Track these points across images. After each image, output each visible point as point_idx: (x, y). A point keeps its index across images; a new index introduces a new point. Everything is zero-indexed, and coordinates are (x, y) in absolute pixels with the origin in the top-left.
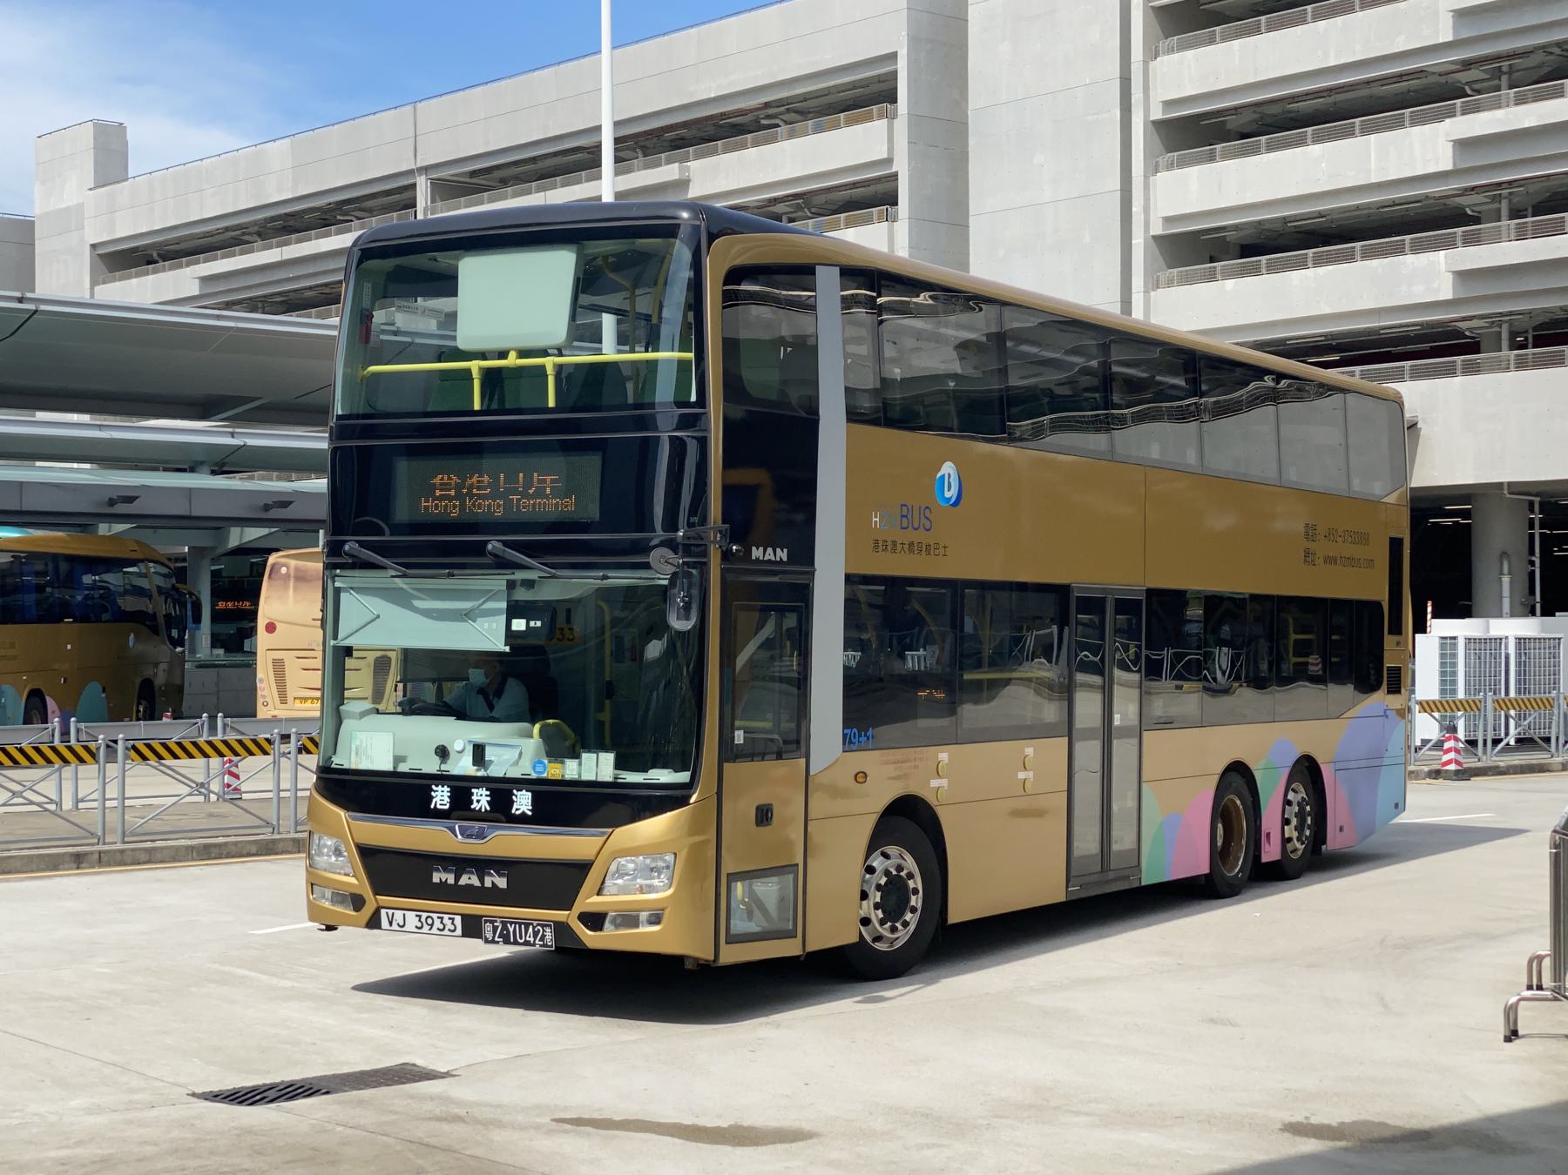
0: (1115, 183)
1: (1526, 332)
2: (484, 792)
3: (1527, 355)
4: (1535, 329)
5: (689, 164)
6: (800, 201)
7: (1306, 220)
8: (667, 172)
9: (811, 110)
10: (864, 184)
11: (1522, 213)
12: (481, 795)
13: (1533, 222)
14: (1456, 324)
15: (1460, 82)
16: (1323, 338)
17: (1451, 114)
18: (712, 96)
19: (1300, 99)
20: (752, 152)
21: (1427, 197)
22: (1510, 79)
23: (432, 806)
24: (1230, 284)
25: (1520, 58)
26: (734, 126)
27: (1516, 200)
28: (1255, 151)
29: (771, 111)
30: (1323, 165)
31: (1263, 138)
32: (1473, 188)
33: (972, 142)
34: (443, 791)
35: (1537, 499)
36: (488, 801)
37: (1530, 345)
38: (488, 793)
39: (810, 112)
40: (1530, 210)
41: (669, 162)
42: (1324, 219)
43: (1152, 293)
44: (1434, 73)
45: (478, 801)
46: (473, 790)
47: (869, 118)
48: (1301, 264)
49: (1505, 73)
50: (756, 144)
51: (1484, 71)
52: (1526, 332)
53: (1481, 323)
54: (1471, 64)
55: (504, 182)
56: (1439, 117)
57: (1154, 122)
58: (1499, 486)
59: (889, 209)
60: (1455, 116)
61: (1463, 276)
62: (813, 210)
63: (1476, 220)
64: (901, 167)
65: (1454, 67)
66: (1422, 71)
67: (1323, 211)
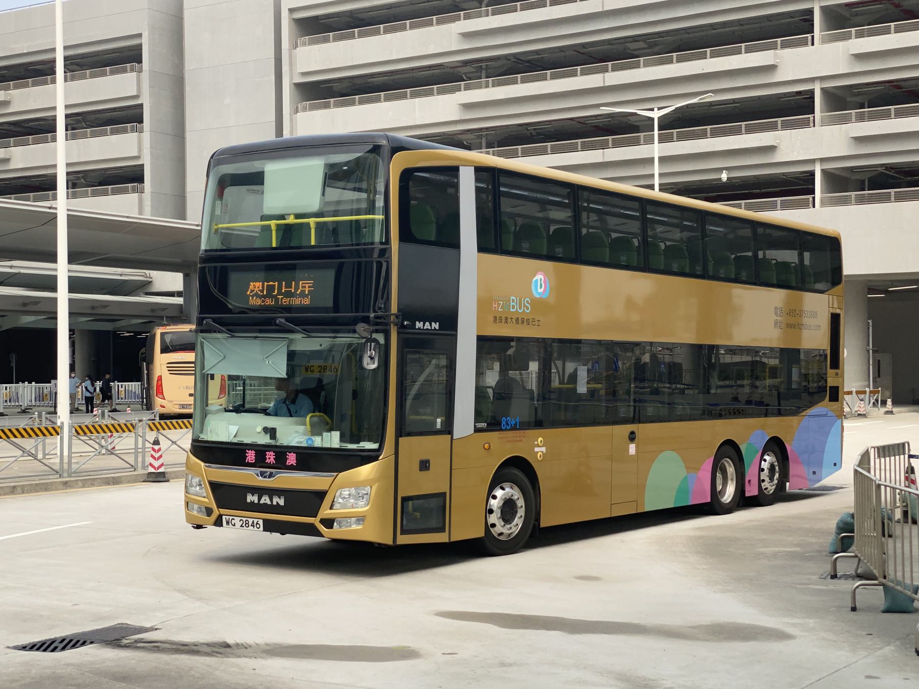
0: (272, 117)
2: (273, 454)
9: (86, 64)
10: (121, 109)
15: (460, 72)
21: (444, 134)
22: (486, 73)
28: (352, 103)
30: (390, 113)
32: (468, 130)
33: (188, 89)
36: (274, 458)
38: (274, 454)
40: (496, 143)
44: (447, 67)
45: (269, 458)
46: (267, 453)
47: (124, 71)
51: (474, 67)
54: (467, 63)
59: (138, 125)
60: (461, 91)
62: (88, 123)
64: (146, 101)
65: (459, 64)
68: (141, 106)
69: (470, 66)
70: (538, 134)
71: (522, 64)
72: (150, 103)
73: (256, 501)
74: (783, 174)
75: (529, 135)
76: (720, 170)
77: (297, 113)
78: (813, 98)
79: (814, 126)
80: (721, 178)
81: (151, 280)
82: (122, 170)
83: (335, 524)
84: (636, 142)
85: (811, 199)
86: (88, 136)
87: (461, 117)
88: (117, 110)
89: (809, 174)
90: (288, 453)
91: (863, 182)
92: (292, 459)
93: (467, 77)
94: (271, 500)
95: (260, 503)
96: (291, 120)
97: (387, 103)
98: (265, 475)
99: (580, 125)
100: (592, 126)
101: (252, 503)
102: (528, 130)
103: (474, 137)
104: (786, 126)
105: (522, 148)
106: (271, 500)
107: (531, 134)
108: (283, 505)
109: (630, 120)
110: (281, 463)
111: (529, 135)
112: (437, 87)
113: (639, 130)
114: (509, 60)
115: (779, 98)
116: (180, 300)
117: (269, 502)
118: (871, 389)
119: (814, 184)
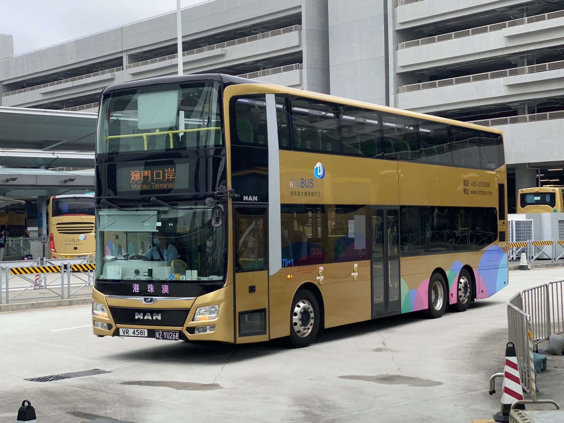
0: (383, 54)
1: (534, 107)
2: (152, 286)
3: (535, 115)
5: (225, 48)
6: (267, 62)
8: (217, 51)
10: (290, 55)
11: (532, 63)
12: (151, 287)
13: (536, 66)
14: (509, 104)
15: (508, 14)
16: (460, 111)
17: (504, 26)
18: (233, 22)
19: (450, 21)
20: (248, 43)
21: (496, 57)
22: (527, 13)
23: (133, 291)
25: (529, 5)
26: (241, 33)
28: (433, 41)
29: (254, 28)
31: (436, 36)
32: (514, 54)
34: (136, 286)
35: (539, 169)
37: (536, 112)
38: (153, 286)
39: (270, 28)
40: (535, 61)
41: (217, 48)
42: (459, 66)
43: (397, 95)
44: (498, 11)
46: (148, 285)
47: (291, 30)
48: (451, 83)
49: (525, 11)
50: (250, 40)
51: (517, 10)
52: (534, 107)
54: (513, 7)
55: (156, 56)
56: (500, 28)
57: (396, 31)
58: (524, 164)
59: (299, 64)
61: (511, 86)
62: (272, 65)
63: (515, 66)
64: (304, 49)
66: (495, 11)
68: (301, 52)
69: (514, 9)
71: (551, 5)
73: (142, 318)
75: (557, 54)
77: (398, 50)
83: (196, 330)
86: (270, 73)
88: (288, 55)
90: (162, 285)
92: (165, 289)
93: (513, 17)
94: (152, 317)
95: (146, 318)
98: (147, 300)
101: (139, 319)
102: (556, 51)
103: (519, 58)
105: (549, 64)
106: (152, 317)
107: (558, 53)
108: (160, 319)
110: (158, 293)
111: (557, 54)
112: (490, 26)
114: (541, 3)
117: (150, 318)
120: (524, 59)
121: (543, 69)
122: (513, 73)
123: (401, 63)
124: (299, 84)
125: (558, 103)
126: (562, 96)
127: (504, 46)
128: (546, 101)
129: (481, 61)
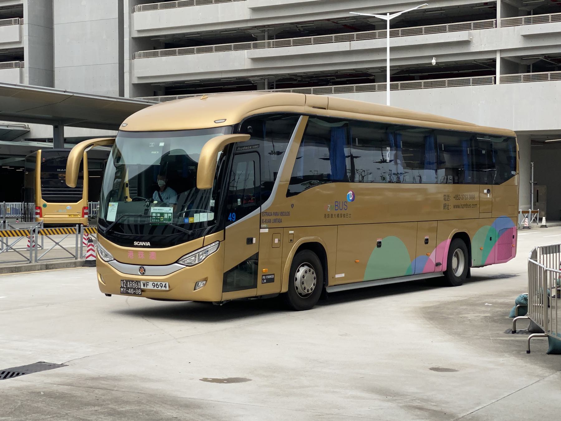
0: (116, 15)
1: (273, 82)
4: (276, 81)
7: (192, 35)
10: (6, 8)
21: (238, 29)
24: (164, 58)
27: (270, 32)
30: (200, 14)
32: (255, 27)
37: (275, 88)
40: (275, 36)
42: (199, 35)
43: (133, 60)
48: (192, 52)
52: (273, 82)
53: (258, 78)
59: (19, 19)
61: (255, 60)
63: (256, 39)
67: (199, 32)
70: (305, 30)
72: (28, 4)
74: (474, 60)
75: (298, 30)
76: (431, 57)
78: (496, 7)
79: (496, 27)
80: (432, 63)
81: (29, 130)
82: (7, 51)
84: (373, 37)
85: (493, 78)
87: (250, 17)
88: (5, 8)
89: (492, 61)
91: (529, 66)
96: (130, 18)
97: (198, 7)
99: (334, 24)
100: (342, 25)
102: (297, 27)
104: (477, 27)
107: (299, 29)
109: (368, 21)
113: (375, 28)
115: (472, 7)
116: (51, 145)
118: (533, 210)
119: (495, 68)
120: (265, 33)
121: (288, 44)
122: (255, 47)
123: (138, 26)
124: (18, 40)
125: (296, 80)
126: (305, 73)
127: (248, 17)
128: (288, 77)
129: (222, 32)
